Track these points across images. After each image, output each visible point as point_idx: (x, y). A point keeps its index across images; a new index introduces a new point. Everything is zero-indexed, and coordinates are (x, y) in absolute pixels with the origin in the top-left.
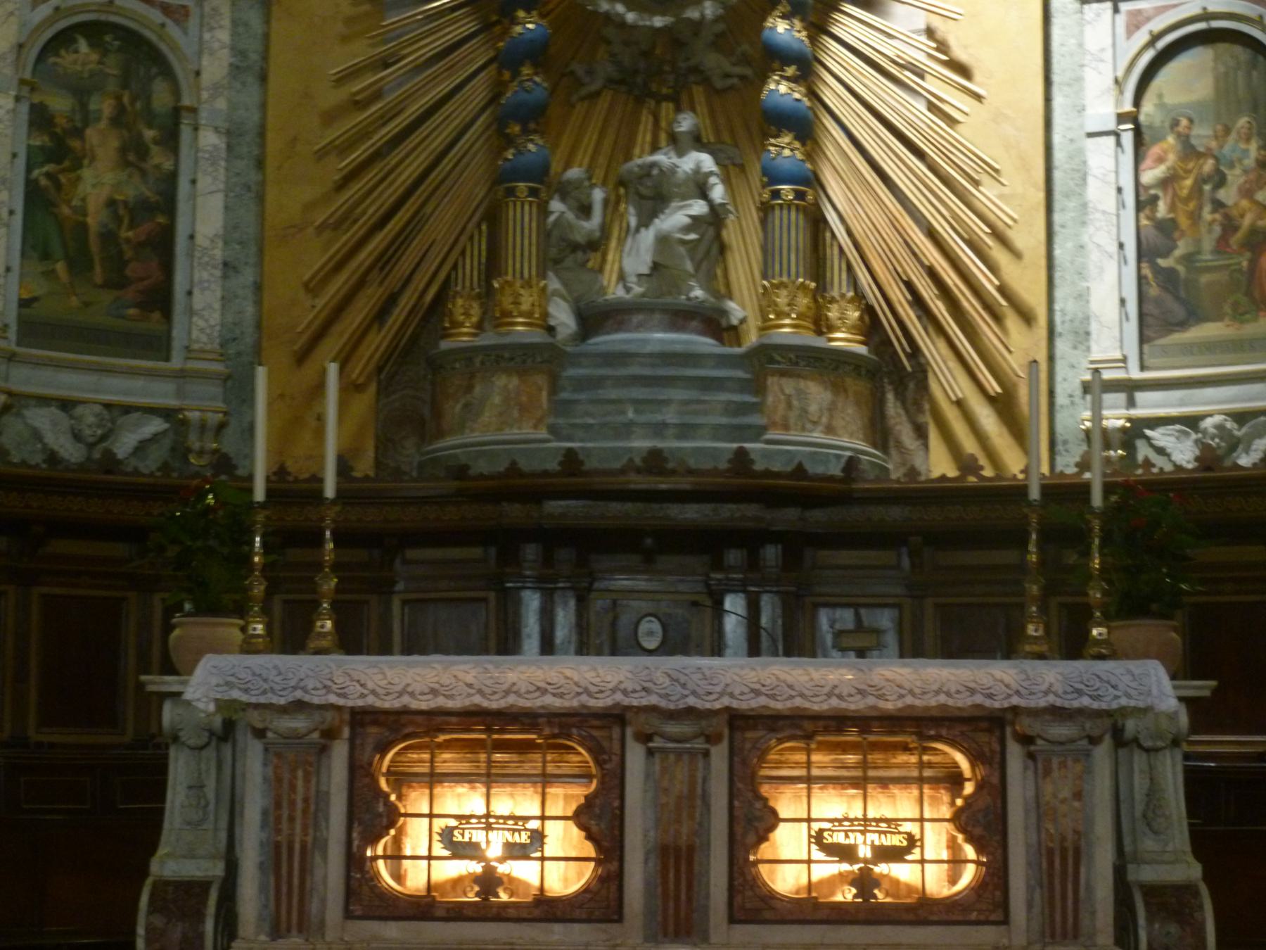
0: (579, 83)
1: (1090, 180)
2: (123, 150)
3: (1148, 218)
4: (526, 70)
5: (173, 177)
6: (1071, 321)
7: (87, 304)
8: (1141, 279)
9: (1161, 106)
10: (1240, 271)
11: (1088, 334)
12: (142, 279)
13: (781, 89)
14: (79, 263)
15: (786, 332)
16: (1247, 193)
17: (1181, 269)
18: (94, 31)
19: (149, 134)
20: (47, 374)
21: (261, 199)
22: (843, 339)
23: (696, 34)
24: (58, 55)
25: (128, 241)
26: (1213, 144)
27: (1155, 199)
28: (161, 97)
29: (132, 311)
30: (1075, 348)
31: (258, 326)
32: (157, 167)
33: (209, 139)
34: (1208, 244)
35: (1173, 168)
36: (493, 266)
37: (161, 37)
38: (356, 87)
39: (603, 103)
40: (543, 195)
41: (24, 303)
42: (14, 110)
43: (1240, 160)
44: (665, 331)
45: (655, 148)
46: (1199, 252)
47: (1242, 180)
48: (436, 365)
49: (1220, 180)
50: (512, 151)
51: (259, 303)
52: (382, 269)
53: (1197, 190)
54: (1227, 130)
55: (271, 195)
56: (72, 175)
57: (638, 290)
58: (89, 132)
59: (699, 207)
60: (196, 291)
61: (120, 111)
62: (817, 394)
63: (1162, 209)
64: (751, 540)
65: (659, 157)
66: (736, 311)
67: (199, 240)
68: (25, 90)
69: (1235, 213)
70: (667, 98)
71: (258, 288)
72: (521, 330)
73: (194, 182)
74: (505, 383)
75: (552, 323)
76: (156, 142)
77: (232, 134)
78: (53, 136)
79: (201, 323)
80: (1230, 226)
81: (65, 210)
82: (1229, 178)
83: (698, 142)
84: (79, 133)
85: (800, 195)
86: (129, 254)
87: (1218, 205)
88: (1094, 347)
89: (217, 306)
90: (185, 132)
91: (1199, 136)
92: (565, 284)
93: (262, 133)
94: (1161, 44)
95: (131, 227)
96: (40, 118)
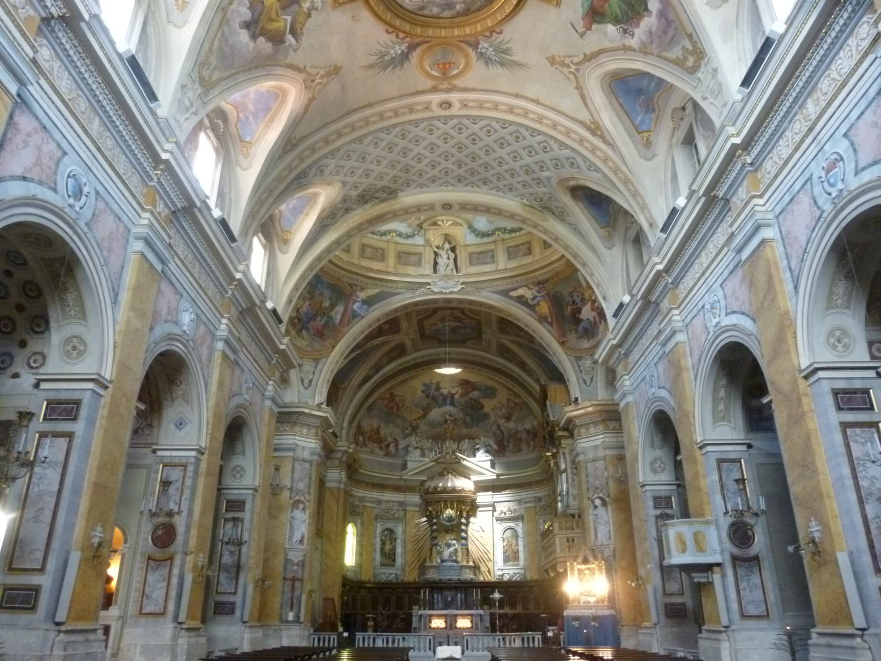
13: (463, 534)
14: (386, 556)
15: (464, 563)
18: (387, 529)
22: (471, 564)
36: (431, 555)
48: (425, 567)
62: (468, 571)
64: (461, 588)
66: (459, 559)
72: (434, 564)
74: (432, 570)
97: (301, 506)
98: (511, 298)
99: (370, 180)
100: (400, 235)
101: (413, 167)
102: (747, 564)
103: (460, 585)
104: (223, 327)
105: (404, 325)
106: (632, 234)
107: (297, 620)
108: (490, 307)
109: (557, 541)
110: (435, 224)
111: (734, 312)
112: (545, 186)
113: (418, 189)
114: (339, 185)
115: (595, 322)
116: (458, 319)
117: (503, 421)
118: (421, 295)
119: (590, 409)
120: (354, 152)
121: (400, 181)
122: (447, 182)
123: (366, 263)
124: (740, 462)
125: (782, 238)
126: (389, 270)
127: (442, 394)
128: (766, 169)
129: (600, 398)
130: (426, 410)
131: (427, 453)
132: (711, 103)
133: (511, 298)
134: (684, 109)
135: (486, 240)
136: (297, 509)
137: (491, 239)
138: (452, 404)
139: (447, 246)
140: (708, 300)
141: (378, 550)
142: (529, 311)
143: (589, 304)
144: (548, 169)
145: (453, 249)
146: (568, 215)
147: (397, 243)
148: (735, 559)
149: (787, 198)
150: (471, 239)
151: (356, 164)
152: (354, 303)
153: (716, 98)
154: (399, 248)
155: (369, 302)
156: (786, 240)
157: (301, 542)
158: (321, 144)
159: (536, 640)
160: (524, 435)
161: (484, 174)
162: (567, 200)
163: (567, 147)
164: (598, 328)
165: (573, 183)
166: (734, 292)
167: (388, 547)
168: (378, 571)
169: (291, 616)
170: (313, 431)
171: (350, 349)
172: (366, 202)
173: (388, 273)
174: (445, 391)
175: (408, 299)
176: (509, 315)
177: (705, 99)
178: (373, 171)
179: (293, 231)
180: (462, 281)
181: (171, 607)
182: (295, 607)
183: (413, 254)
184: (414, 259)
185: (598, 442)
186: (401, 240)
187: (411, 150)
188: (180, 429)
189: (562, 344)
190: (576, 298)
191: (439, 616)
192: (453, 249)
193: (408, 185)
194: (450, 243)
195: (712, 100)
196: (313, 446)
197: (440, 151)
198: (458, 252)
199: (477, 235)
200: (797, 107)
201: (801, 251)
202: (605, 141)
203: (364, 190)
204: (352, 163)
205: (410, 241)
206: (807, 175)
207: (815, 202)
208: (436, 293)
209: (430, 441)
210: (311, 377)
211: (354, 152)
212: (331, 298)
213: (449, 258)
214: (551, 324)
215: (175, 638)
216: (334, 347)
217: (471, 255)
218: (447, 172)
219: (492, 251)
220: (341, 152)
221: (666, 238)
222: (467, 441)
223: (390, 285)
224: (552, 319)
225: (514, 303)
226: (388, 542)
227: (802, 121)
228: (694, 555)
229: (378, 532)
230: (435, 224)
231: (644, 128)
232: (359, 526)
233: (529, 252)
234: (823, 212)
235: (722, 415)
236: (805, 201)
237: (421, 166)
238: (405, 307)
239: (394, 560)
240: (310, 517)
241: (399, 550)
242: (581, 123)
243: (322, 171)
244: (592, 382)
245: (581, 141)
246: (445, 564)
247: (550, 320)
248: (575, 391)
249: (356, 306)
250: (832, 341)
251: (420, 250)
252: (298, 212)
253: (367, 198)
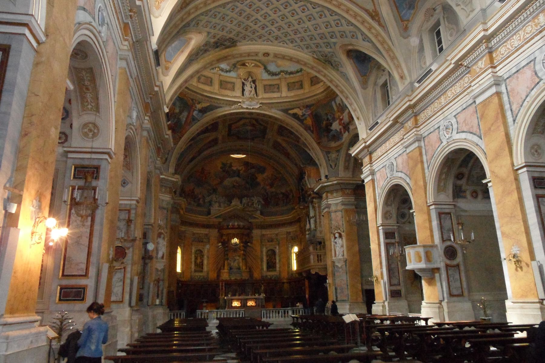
77: (207, 256)
96: (195, 256)
97: (162, 236)
98: (289, 114)
99: (224, 33)
100: (222, 70)
101: (251, 27)
102: (453, 268)
104: (146, 121)
105: (220, 127)
106: (381, 81)
107: (161, 304)
108: (276, 119)
109: (312, 257)
110: (244, 65)
111: (463, 132)
112: (331, 48)
113: (250, 42)
114: (206, 34)
115: (341, 132)
116: (253, 125)
117: (268, 187)
118: (235, 109)
119: (335, 182)
120: (219, 13)
121: (241, 35)
122: (269, 39)
123: (201, 86)
124: (451, 215)
125: (507, 93)
126: (215, 91)
127: (233, 170)
128: (500, 52)
129: (340, 176)
130: (222, 179)
131: (222, 205)
132: (462, 9)
133: (289, 114)
134: (434, 10)
135: (274, 77)
136: (160, 237)
137: (277, 77)
138: (238, 176)
139: (250, 79)
140: (442, 124)
141: (193, 263)
142: (299, 123)
143: (338, 121)
144: (336, 37)
145: (254, 82)
146: (342, 67)
147: (220, 75)
148: (447, 266)
149: (514, 70)
150: (265, 76)
151: (218, 21)
152: (193, 111)
153: (466, 6)
154: (221, 78)
155: (203, 111)
156: (510, 94)
157: (163, 257)
158: (202, 5)
159: (301, 312)
160: (281, 196)
161: (293, 36)
162: (343, 58)
163: (352, 24)
164: (342, 135)
165: (350, 47)
166: (465, 121)
167: (199, 261)
168: (192, 274)
169: (158, 302)
170: (168, 189)
171: (189, 140)
172: (217, 47)
173: (216, 94)
174: (234, 168)
175: (226, 111)
176: (287, 124)
177: (458, 5)
178: (227, 27)
179: (172, 62)
180: (260, 102)
181: (127, 297)
182: (160, 297)
183: (229, 83)
184: (229, 86)
185: (339, 201)
186: (222, 73)
187: (252, 16)
188: (124, 186)
189: (319, 144)
190: (329, 117)
191: (251, 299)
192: (254, 82)
193: (245, 38)
194: (252, 78)
195: (462, 7)
196: (168, 199)
197: (270, 18)
198: (257, 84)
199: (269, 74)
200: (531, 17)
201: (520, 101)
202: (380, 24)
203: (218, 39)
204: (217, 20)
205: (228, 74)
206: (532, 57)
207: (536, 74)
208: (244, 108)
209: (224, 197)
210: (166, 156)
211: (219, 13)
212: (180, 107)
213: (252, 87)
214: (312, 132)
215: (131, 315)
216: (181, 138)
217: (265, 86)
218: (270, 33)
219: (278, 85)
220: (212, 13)
221: (419, 87)
222: (246, 198)
223: (216, 101)
224: (313, 128)
225: (290, 117)
226: (199, 258)
227: (533, 26)
228: (414, 264)
229: (193, 251)
230: (244, 65)
231: (405, 18)
232: (182, 248)
233: (301, 87)
234: (541, 80)
235: (442, 188)
236: (528, 73)
237: (256, 27)
238: (225, 115)
239: (202, 268)
240: (167, 243)
241: (205, 262)
242: (367, 11)
243: (198, 24)
244: (335, 166)
245: (363, 22)
247: (312, 129)
248: (324, 171)
249: (195, 113)
250: (533, 151)
251: (233, 80)
252: (179, 50)
253: (219, 44)
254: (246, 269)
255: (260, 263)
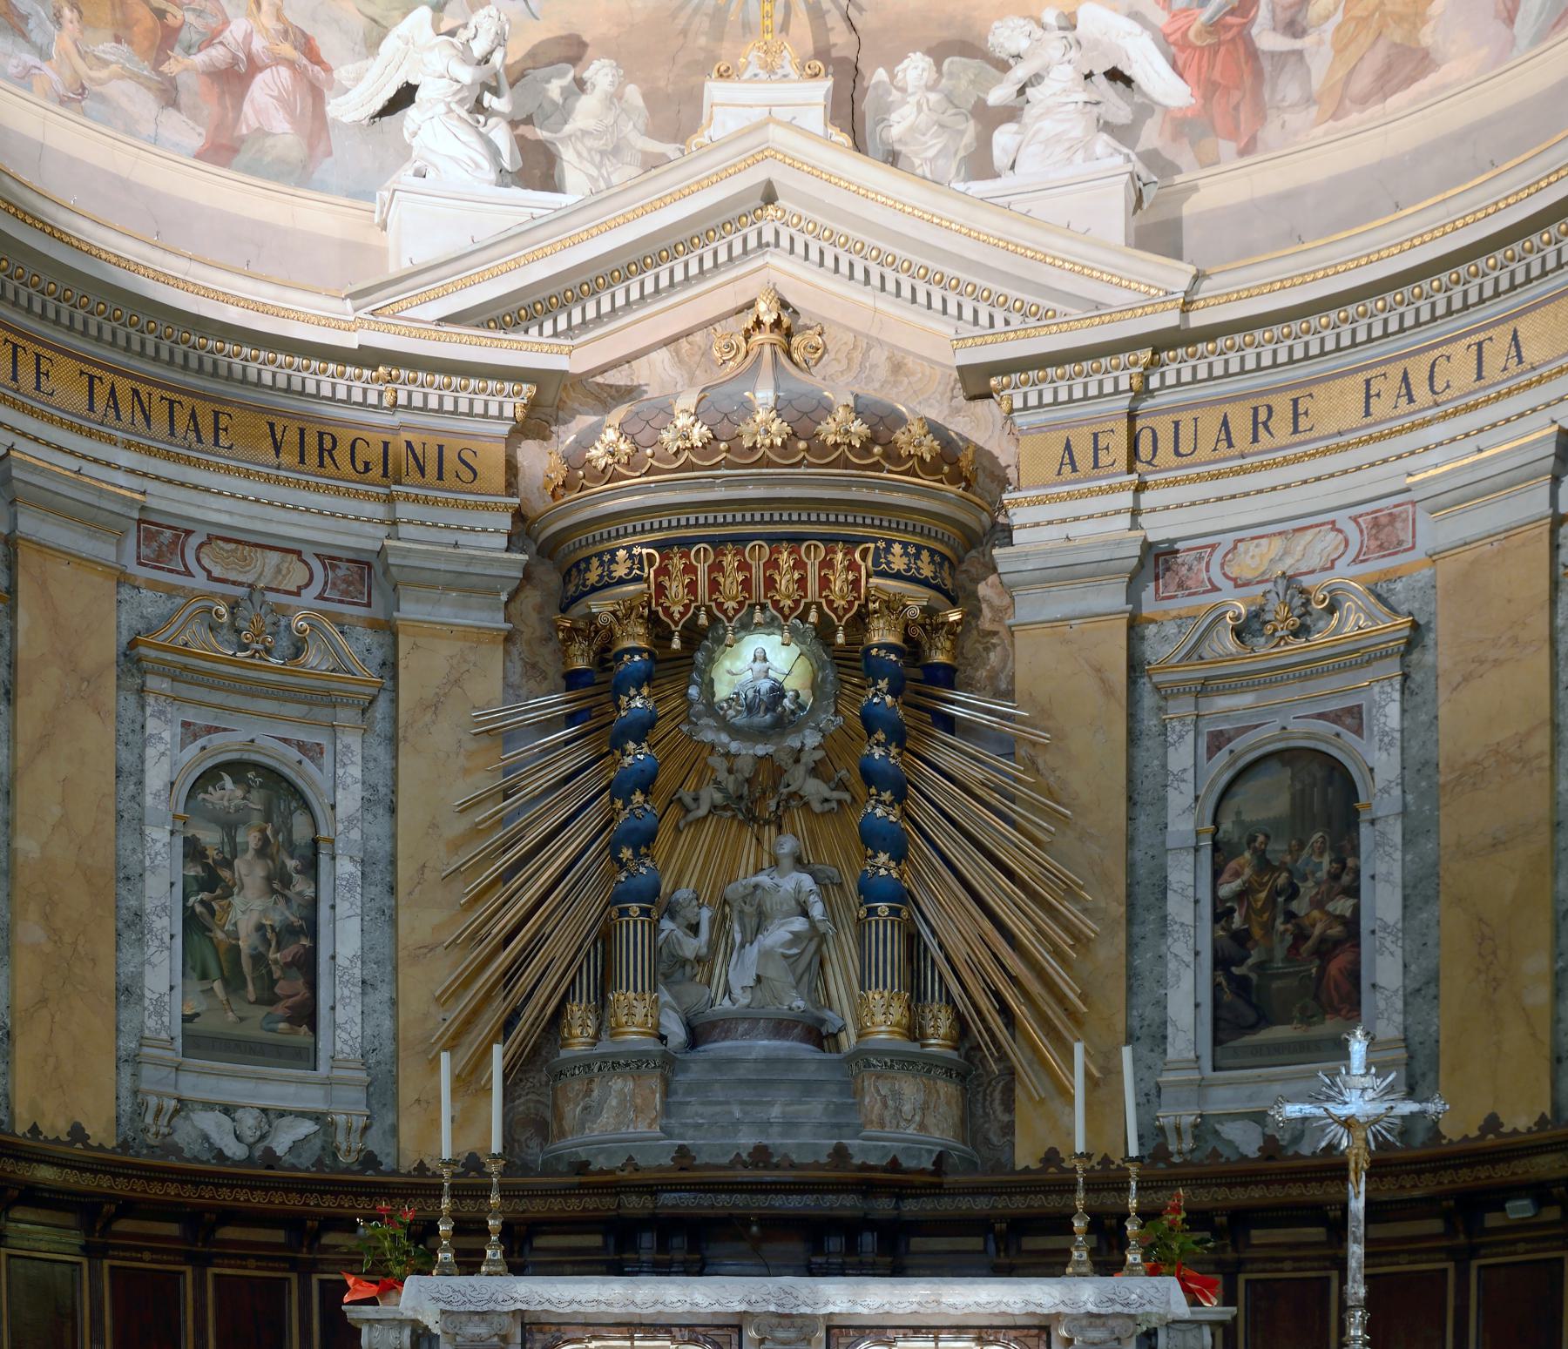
0: (688, 811)
1: (1170, 893)
2: (269, 879)
3: (1223, 929)
4: (638, 797)
5: (314, 903)
6: (1149, 1026)
7: (241, 1019)
8: (1216, 987)
9: (1239, 822)
10: (1310, 976)
11: (1165, 1037)
12: (289, 997)
16: (1318, 904)
17: (1253, 976)
19: (291, 864)
20: (211, 1081)
21: (393, 922)
23: (797, 761)
24: (206, 792)
25: (276, 962)
26: (1288, 858)
27: (1231, 911)
28: (301, 829)
29: (282, 1026)
30: (1152, 1050)
31: (395, 1038)
32: (300, 894)
33: (346, 867)
34: (1280, 952)
35: (1248, 881)
37: (297, 773)
38: (480, 815)
39: (709, 828)
40: (654, 914)
41: (187, 1019)
42: (170, 843)
43: (1313, 873)
44: (769, 1039)
45: (758, 870)
46: (1271, 960)
47: (1314, 892)
49: (1293, 892)
50: (624, 874)
51: (395, 1017)
52: (505, 986)
53: (1271, 900)
54: (1302, 845)
55: (403, 920)
56: (224, 902)
57: (744, 1000)
58: (236, 862)
59: (799, 924)
60: (339, 1007)
61: (265, 841)
63: (1237, 921)
65: (763, 878)
67: (339, 960)
68: (179, 823)
69: (1307, 922)
70: (768, 822)
71: (394, 1003)
73: (333, 907)
75: (664, 1033)
76: (298, 872)
78: (206, 867)
79: (344, 1036)
80: (1301, 936)
81: (220, 935)
82: (1302, 890)
83: (799, 863)
84: (229, 864)
85: (895, 912)
86: (277, 974)
87: (1290, 916)
88: (1170, 1050)
89: (358, 1020)
90: (324, 860)
91: (1275, 851)
92: (676, 997)
93: (393, 861)
94: (1241, 763)
95: (278, 949)
96: (193, 850)
103: (847, 1204)
226: (249, 872)
246: (720, 1047)
254: (914, 1031)
255: (1110, 952)
